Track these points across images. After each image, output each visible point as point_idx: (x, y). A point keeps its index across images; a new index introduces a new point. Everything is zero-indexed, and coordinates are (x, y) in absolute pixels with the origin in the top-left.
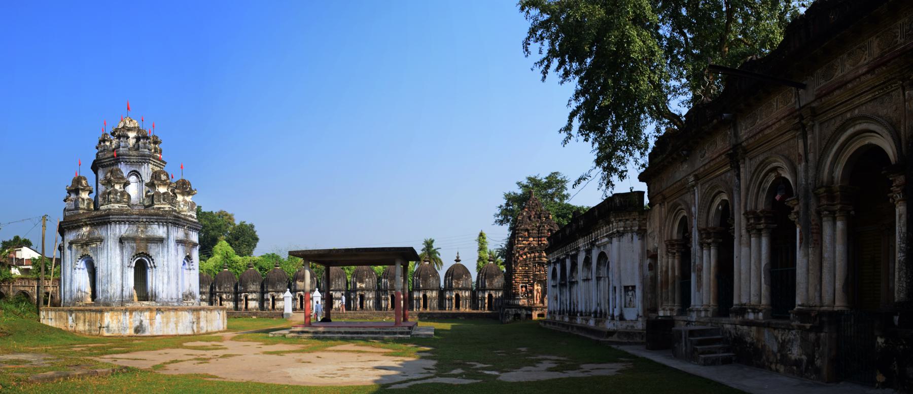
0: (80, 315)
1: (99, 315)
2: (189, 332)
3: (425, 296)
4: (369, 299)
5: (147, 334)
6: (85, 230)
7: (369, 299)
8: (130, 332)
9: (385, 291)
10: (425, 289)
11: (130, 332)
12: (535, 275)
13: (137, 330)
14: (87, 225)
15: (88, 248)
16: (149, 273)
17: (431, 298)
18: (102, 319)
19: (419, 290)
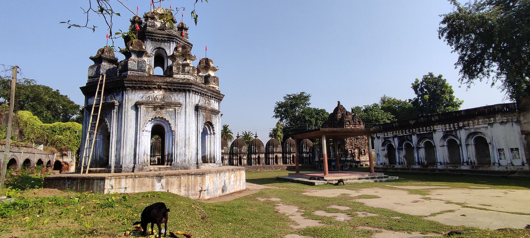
0: (174, 180)
1: (199, 178)
2: (245, 188)
3: (259, 157)
4: (226, 159)
5: (228, 192)
6: (158, 94)
7: (226, 159)
8: (219, 193)
9: (236, 154)
10: (259, 153)
11: (219, 193)
12: (355, 144)
13: (223, 191)
14: (160, 88)
15: (164, 111)
16: (208, 138)
17: (262, 158)
18: (203, 182)
19: (255, 153)
